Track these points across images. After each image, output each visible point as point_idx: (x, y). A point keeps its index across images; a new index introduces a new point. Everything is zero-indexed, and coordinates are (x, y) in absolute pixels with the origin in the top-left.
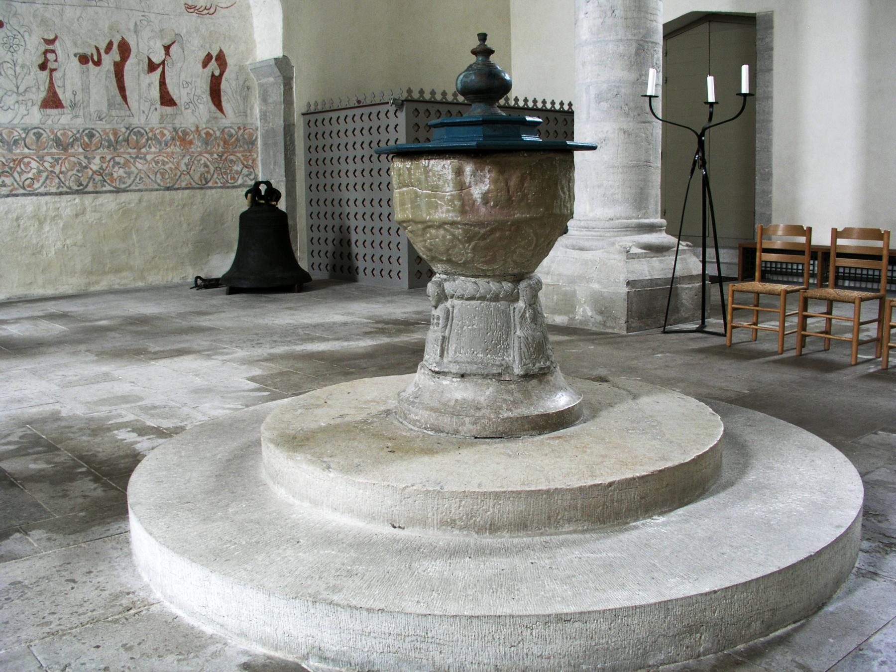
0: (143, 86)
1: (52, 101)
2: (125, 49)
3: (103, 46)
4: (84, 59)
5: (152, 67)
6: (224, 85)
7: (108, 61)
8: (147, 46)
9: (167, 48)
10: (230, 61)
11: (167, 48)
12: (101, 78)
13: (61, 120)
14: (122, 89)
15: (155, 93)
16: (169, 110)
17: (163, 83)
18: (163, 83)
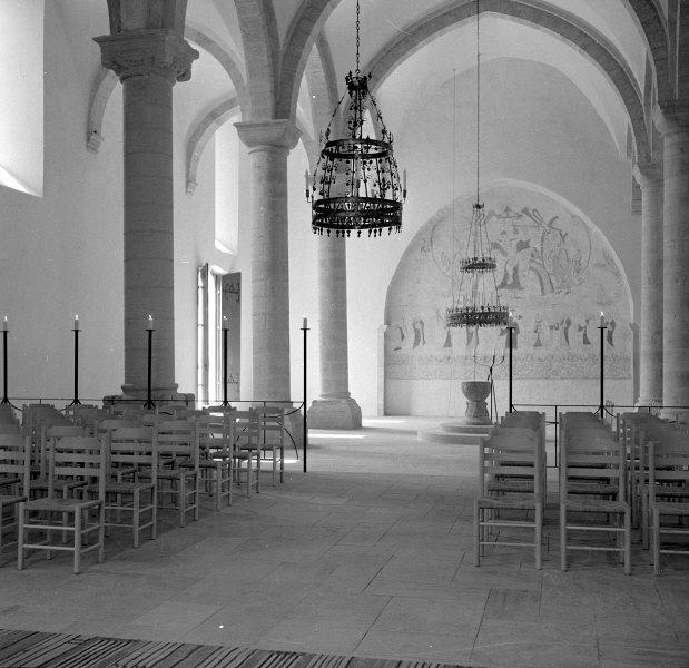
0: (575, 336)
1: (538, 344)
2: (569, 322)
3: (559, 322)
4: (551, 328)
5: (580, 329)
6: (614, 335)
7: (561, 328)
8: (576, 321)
9: (587, 321)
10: (618, 323)
11: (587, 321)
12: (558, 334)
13: (542, 351)
14: (567, 338)
15: (582, 340)
16: (588, 346)
17: (585, 335)
18: (585, 335)
